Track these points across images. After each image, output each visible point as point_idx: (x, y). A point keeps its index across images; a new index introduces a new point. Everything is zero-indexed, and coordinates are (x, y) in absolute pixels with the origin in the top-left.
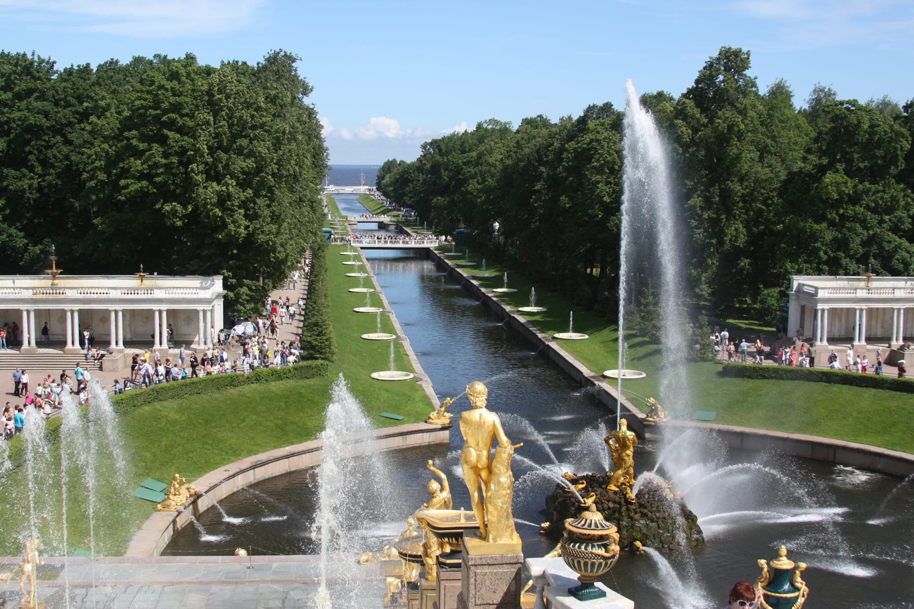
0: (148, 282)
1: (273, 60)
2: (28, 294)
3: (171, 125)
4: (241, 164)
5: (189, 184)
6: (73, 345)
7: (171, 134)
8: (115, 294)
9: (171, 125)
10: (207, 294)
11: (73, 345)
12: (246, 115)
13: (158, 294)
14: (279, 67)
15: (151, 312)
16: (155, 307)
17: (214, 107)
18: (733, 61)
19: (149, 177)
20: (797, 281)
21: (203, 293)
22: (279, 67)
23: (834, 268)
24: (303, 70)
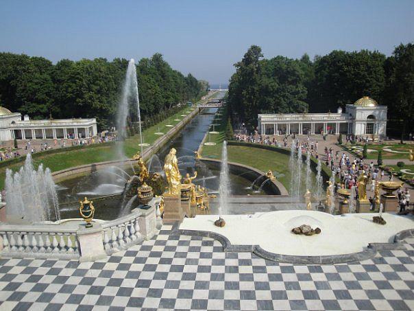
0: (75, 120)
1: (155, 56)
2: (43, 125)
3: (78, 78)
4: (95, 88)
5: (83, 94)
6: (55, 138)
7: (77, 81)
8: (64, 124)
9: (78, 78)
10: (88, 123)
11: (55, 138)
12: (97, 74)
13: (75, 124)
14: (157, 58)
15: (73, 129)
16: (74, 127)
17: (89, 73)
18: (255, 50)
19: (73, 92)
20: (259, 115)
21: (89, 123)
22: (157, 58)
23: (276, 111)
24: (165, 59)
